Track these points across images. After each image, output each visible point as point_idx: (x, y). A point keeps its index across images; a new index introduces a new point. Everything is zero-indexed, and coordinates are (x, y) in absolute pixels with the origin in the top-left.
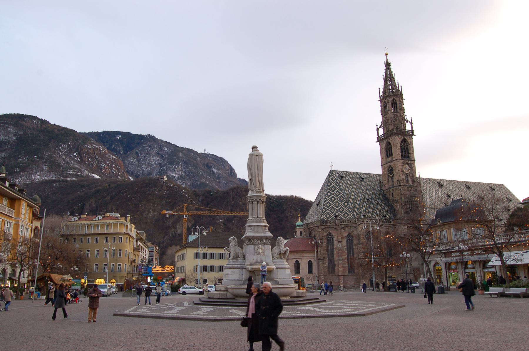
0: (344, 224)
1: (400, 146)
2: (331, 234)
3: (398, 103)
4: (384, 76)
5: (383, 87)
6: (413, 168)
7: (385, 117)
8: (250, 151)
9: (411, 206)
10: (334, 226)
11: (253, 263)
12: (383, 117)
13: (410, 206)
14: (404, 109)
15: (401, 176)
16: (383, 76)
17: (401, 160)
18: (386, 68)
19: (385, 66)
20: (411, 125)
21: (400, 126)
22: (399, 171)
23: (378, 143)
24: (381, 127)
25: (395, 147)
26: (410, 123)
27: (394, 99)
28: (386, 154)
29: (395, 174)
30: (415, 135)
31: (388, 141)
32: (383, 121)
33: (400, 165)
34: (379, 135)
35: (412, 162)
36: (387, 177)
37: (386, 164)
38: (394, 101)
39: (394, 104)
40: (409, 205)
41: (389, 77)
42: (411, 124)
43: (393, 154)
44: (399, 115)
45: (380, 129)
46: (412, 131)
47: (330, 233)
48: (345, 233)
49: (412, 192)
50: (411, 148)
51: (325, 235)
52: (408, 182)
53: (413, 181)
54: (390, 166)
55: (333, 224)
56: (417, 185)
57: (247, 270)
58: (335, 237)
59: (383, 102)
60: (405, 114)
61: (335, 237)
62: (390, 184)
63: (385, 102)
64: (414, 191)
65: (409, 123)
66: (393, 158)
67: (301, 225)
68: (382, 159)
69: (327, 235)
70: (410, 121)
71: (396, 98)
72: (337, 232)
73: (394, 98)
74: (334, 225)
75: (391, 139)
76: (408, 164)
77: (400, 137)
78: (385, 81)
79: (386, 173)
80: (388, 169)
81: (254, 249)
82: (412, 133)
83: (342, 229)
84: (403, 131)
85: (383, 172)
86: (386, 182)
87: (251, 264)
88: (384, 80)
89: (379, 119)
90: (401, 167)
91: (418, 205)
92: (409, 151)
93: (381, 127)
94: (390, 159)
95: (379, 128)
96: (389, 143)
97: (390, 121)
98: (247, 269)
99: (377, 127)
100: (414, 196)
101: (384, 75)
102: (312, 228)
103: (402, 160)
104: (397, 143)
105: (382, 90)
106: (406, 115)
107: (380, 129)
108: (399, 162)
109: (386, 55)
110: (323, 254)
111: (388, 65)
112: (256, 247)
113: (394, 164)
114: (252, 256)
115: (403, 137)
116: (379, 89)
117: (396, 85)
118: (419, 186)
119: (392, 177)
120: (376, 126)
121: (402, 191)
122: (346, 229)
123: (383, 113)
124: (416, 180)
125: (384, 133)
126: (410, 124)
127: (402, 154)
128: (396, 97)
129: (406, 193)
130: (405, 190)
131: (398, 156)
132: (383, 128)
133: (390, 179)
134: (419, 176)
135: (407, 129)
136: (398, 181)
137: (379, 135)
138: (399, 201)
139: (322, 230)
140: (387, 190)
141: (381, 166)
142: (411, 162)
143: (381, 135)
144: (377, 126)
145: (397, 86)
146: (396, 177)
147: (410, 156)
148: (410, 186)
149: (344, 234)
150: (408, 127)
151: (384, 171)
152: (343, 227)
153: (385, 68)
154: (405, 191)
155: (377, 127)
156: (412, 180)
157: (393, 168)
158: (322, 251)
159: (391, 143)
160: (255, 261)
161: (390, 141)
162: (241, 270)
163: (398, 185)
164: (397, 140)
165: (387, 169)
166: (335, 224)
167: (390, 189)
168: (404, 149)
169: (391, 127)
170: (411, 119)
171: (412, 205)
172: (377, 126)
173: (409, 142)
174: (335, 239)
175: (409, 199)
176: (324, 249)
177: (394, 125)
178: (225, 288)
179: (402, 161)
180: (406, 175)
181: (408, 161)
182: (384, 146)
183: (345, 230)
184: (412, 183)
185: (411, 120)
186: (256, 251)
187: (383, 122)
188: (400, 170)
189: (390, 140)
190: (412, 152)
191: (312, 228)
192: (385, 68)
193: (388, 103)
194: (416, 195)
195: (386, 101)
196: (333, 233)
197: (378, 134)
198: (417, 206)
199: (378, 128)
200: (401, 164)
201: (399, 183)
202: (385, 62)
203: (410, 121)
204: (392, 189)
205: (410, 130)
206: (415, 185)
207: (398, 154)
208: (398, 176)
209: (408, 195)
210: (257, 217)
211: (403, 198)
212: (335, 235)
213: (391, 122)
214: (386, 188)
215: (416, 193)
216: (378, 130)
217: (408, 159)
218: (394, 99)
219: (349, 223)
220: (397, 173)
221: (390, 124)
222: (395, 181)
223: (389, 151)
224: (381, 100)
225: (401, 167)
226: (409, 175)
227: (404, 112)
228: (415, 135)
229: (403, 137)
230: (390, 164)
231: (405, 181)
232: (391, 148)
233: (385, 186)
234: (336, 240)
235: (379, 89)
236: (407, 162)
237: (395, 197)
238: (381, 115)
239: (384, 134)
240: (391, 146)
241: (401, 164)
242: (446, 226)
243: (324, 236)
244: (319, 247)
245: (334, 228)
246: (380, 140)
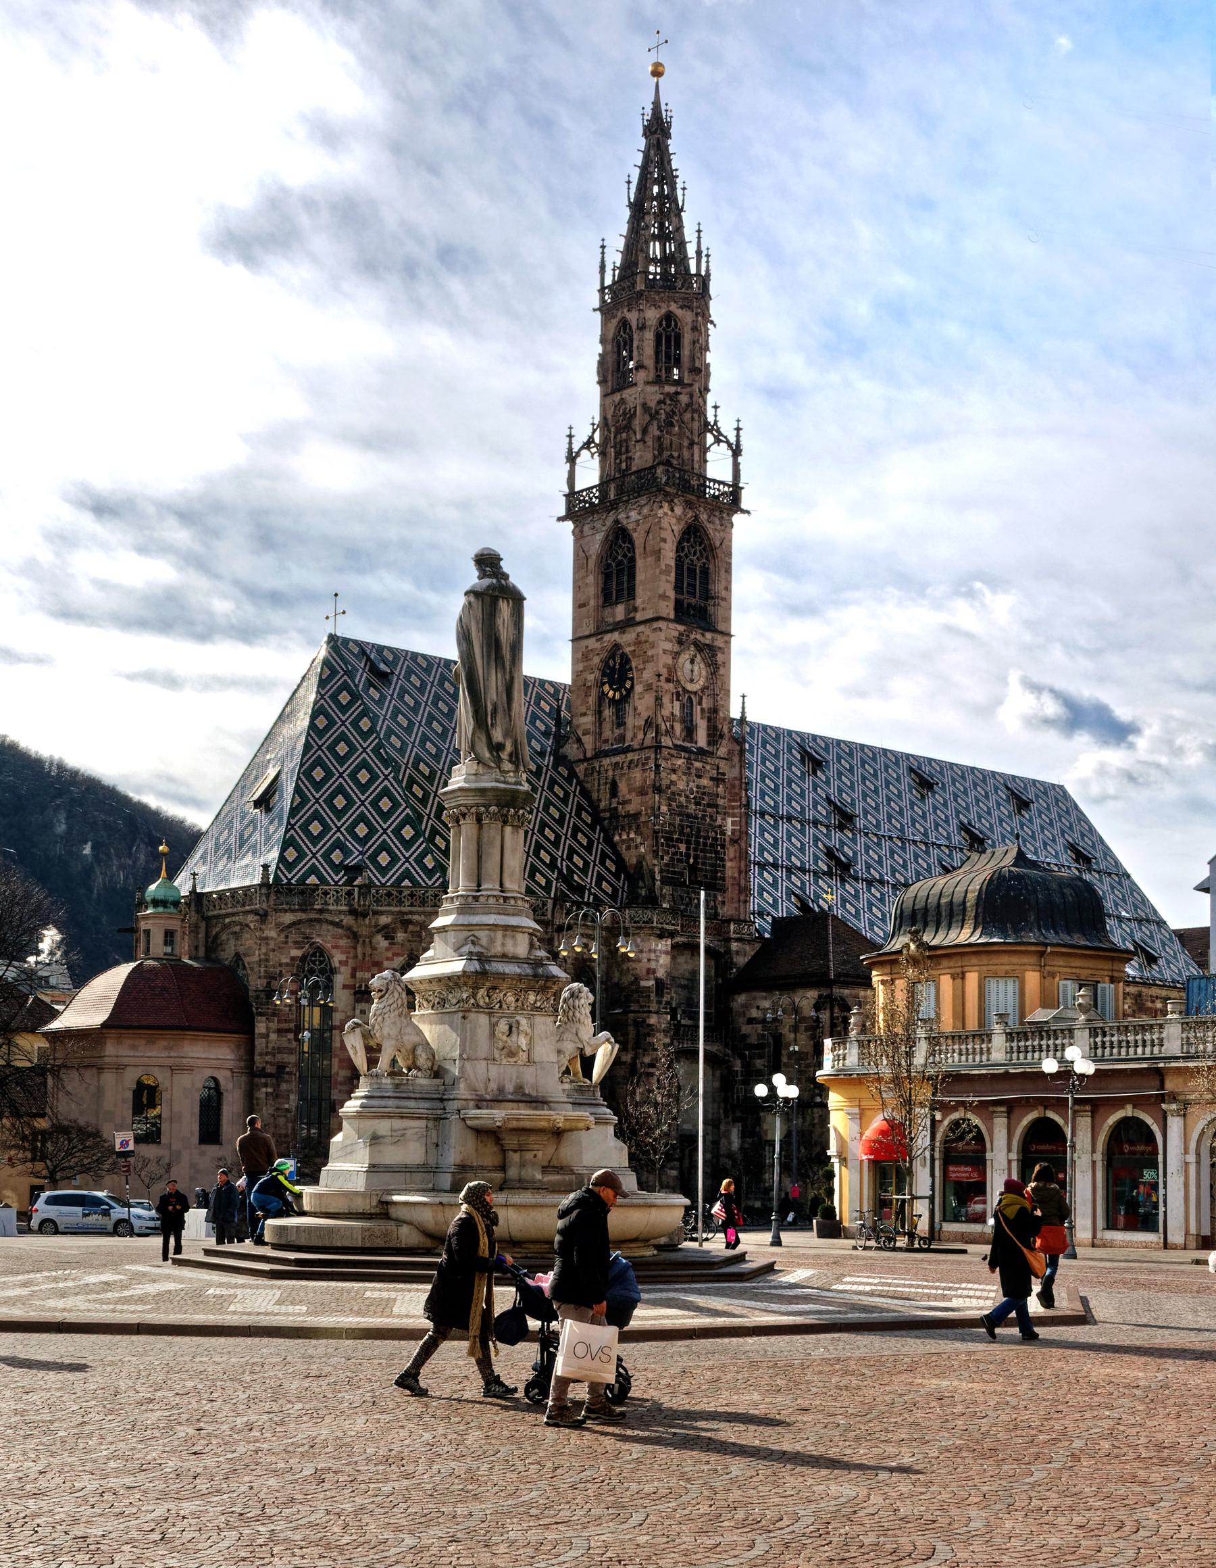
0: (392, 913)
1: (672, 555)
2: (322, 955)
3: (687, 338)
5: (621, 244)
6: (722, 671)
7: (617, 397)
8: (471, 577)
9: (696, 850)
10: (342, 917)
11: (488, 1097)
12: (604, 396)
13: (688, 849)
14: (708, 375)
15: (666, 700)
16: (629, 182)
17: (672, 625)
18: (649, 147)
19: (645, 134)
20: (731, 460)
21: (686, 454)
22: (659, 675)
23: (569, 525)
24: (587, 445)
25: (650, 560)
26: (729, 445)
27: (669, 317)
28: (601, 585)
29: (638, 688)
30: (748, 512)
31: (617, 522)
32: (604, 418)
33: (665, 651)
35: (719, 642)
36: (592, 700)
37: (599, 633)
38: (668, 325)
39: (668, 339)
40: (688, 842)
42: (736, 451)
43: (639, 590)
44: (684, 399)
45: (585, 454)
47: (320, 951)
48: (390, 954)
49: (705, 782)
50: (722, 572)
51: (293, 959)
52: (690, 732)
53: (714, 735)
54: (617, 646)
55: (339, 908)
56: (730, 752)
57: (468, 1127)
58: (343, 969)
59: (615, 322)
60: (711, 399)
61: (343, 969)
62: (607, 734)
63: (624, 324)
64: (712, 779)
65: (724, 446)
66: (635, 609)
67: (171, 899)
68: (579, 605)
69: (303, 959)
70: (733, 440)
71: (679, 312)
72: (355, 948)
73: (673, 307)
74: (340, 912)
76: (700, 647)
78: (638, 209)
79: (591, 677)
80: (605, 662)
81: (493, 1034)
82: (732, 501)
83: (378, 932)
84: (694, 482)
85: (576, 674)
86: (587, 721)
87: (480, 1102)
88: (631, 205)
90: (669, 660)
91: (723, 847)
92: (711, 587)
93: (589, 448)
94: (620, 612)
95: (582, 448)
96: (620, 536)
97: (637, 424)
98: (469, 1122)
99: (570, 443)
100: (709, 805)
102: (227, 920)
103: (681, 628)
104: (664, 540)
105: (615, 258)
106: (716, 407)
107: (585, 453)
108: (662, 635)
110: (280, 1050)
112: (503, 1026)
113: (638, 642)
114: (484, 1063)
115: (690, 514)
116: (603, 247)
117: (682, 245)
118: (736, 759)
119: (620, 705)
120: (567, 440)
121: (663, 775)
122: (400, 936)
123: (610, 377)
124: (726, 730)
125: (601, 477)
126: (730, 453)
127: (679, 597)
128: (681, 308)
129: (681, 785)
130: (674, 771)
131: (663, 604)
132: (603, 454)
133: (608, 713)
134: (743, 712)
135: (709, 475)
136: (649, 723)
138: (643, 819)
139: (282, 930)
140: (586, 759)
141: (572, 641)
142: (713, 640)
144: (570, 436)
145: (691, 250)
146: (642, 703)
147: (711, 609)
148: (701, 752)
149: (388, 959)
150: (718, 466)
151: (581, 667)
152: (386, 927)
153: (643, 141)
154: (674, 777)
155: (570, 443)
156: (709, 728)
157: (628, 661)
158: (273, 1036)
159: (635, 535)
160: (493, 1086)
161: (630, 527)
162: (431, 1124)
164: (665, 523)
165: (596, 660)
166: (344, 908)
167: (606, 761)
168: (692, 571)
169: (641, 457)
170: (738, 429)
171: (697, 843)
172: (570, 436)
173: (718, 543)
174: (339, 980)
175: (689, 816)
176: (285, 1026)
177: (661, 449)
178: (374, 1204)
179: (676, 629)
180: (687, 699)
181: (703, 635)
182: (596, 543)
183: (393, 938)
184: (709, 743)
185: (738, 436)
186: (500, 1045)
187: (604, 424)
188: (664, 672)
189: (631, 517)
190: (723, 593)
191: (227, 920)
192: (642, 143)
193: (642, 328)
194: (721, 802)
195: (633, 317)
196: (334, 951)
197: (571, 480)
198: (717, 852)
199: (576, 448)
200: (668, 646)
201: (651, 734)
203: (733, 440)
204: (614, 759)
205: (720, 483)
206: (722, 751)
207: (664, 597)
208: (649, 699)
209: (687, 797)
210: (497, 887)
211: (664, 809)
212: (340, 962)
213: (645, 431)
214: (585, 753)
215: (721, 789)
216: (572, 458)
217: (702, 624)
218: (669, 317)
219: (414, 909)
220: (649, 688)
221: (639, 437)
222: (633, 721)
223: (619, 572)
224: (606, 310)
225: (669, 660)
226: (700, 703)
227: (707, 390)
228: (748, 512)
229: (690, 514)
230: (615, 636)
231: (678, 728)
232: (633, 560)
233: (579, 741)
234: (345, 987)
235: (603, 247)
236: (699, 637)
237: (628, 802)
239: (603, 486)
240: (632, 549)
241: (668, 646)
242: (945, 963)
243: (287, 965)
244: (261, 1014)
245: (342, 927)
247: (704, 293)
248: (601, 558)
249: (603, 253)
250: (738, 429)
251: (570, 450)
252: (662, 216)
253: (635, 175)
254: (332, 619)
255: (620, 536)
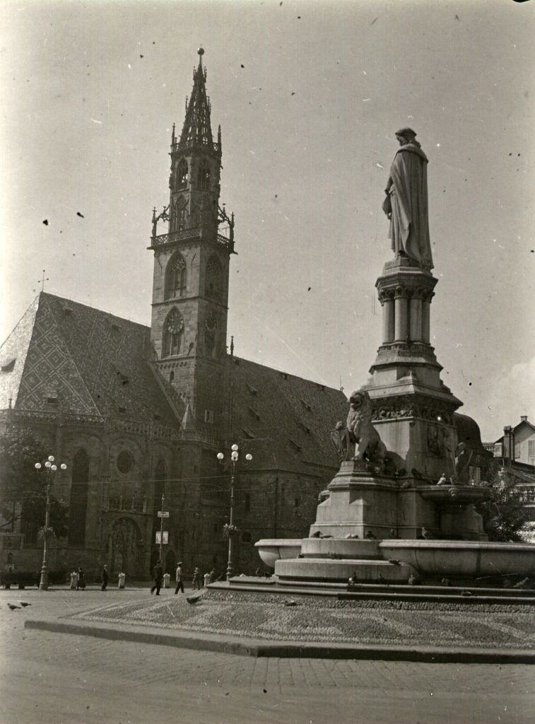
4: (189, 101)
12: (173, 194)
16: (187, 99)
19: (194, 79)
23: (152, 252)
24: (163, 215)
29: (187, 329)
30: (237, 253)
31: (177, 252)
34: (157, 235)
41: (199, 108)
42: (232, 225)
45: (161, 220)
46: (231, 243)
60: (221, 201)
65: (226, 222)
68: (156, 289)
70: (231, 220)
75: (187, 250)
77: (208, 248)
82: (229, 247)
89: (163, 198)
93: (163, 218)
95: (159, 217)
96: (177, 258)
99: (154, 214)
101: (189, 98)
103: (207, 302)
105: (179, 133)
107: (161, 220)
109: (201, 52)
111: (200, 78)
115: (213, 251)
116: (174, 127)
125: (170, 230)
126: (229, 225)
137: (157, 235)
141: (153, 305)
143: (164, 236)
144: (155, 211)
150: (223, 230)
151: (156, 317)
155: (154, 214)
163: (190, 355)
170: (233, 216)
172: (155, 211)
187: (172, 206)
192: (193, 83)
199: (157, 216)
202: (197, 68)
203: (231, 220)
216: (155, 221)
228: (237, 253)
230: (176, 304)
235: (174, 127)
238: (169, 189)
239: (171, 234)
246: (158, 246)
247: (219, 153)
248: (168, 267)
249: (174, 129)
250: (233, 216)
251: (154, 217)
252: (200, 115)
253: (190, 96)
254: (45, 278)
255: (177, 258)
